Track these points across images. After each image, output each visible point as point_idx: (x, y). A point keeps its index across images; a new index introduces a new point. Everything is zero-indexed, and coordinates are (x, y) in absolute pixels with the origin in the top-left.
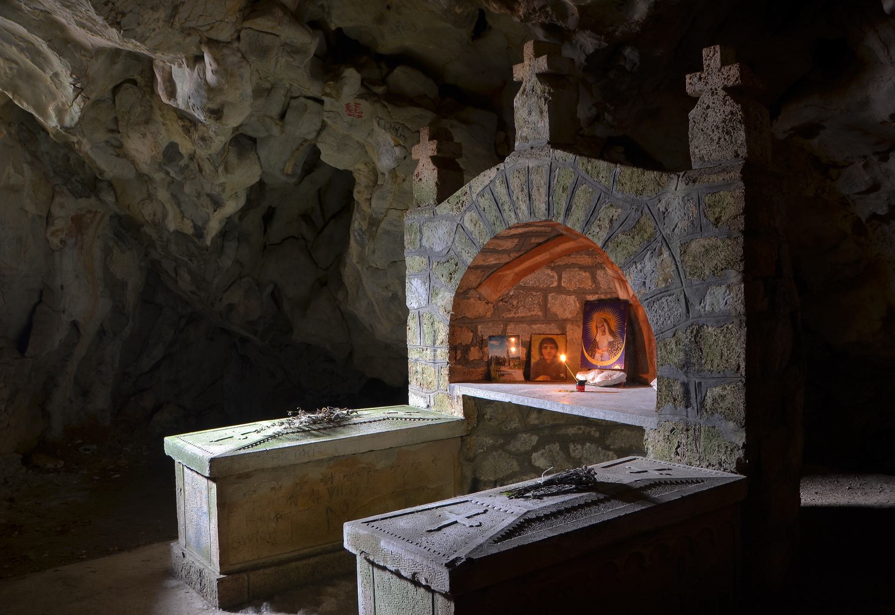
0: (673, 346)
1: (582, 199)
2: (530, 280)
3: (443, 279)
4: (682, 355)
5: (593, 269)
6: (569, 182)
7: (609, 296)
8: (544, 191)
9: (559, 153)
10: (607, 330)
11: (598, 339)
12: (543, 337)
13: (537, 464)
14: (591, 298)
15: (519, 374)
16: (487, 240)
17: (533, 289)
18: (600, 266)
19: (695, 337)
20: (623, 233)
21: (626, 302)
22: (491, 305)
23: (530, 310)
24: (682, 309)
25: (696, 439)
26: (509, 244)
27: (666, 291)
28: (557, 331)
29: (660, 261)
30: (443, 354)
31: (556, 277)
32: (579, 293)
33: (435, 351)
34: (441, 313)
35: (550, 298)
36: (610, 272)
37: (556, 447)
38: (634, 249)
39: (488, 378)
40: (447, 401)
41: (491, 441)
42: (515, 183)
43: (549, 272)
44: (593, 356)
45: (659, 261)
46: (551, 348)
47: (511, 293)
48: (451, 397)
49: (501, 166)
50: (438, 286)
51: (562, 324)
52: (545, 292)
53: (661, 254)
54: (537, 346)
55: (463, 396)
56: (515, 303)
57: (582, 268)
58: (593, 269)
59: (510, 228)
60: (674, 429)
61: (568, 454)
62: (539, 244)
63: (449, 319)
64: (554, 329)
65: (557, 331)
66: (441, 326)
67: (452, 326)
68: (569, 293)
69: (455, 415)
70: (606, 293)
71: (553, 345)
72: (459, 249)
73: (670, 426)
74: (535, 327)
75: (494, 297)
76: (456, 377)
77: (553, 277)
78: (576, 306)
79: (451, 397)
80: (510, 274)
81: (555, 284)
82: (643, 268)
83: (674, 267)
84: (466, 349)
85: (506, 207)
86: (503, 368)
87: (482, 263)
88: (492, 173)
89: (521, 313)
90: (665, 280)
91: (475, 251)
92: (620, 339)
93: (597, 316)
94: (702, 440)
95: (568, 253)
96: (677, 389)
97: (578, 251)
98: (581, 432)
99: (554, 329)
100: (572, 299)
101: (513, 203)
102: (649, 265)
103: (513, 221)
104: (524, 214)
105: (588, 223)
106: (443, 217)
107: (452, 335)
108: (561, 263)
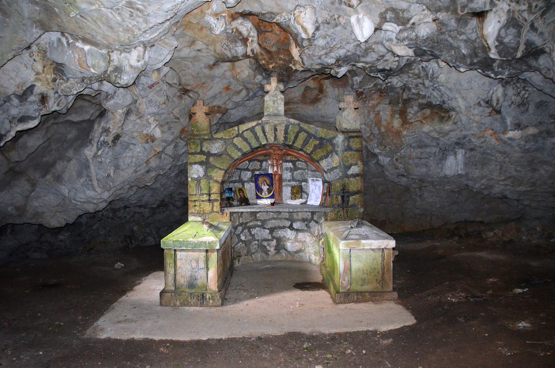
1: (303, 136)
6: (296, 130)
8: (283, 133)
9: (292, 121)
14: (257, 173)
18: (266, 161)
27: (336, 168)
32: (253, 171)
37: (246, 231)
42: (267, 128)
44: (261, 194)
49: (260, 122)
57: (259, 161)
61: (250, 232)
64: (239, 185)
88: (254, 123)
95: (257, 156)
104: (271, 140)
106: (218, 139)
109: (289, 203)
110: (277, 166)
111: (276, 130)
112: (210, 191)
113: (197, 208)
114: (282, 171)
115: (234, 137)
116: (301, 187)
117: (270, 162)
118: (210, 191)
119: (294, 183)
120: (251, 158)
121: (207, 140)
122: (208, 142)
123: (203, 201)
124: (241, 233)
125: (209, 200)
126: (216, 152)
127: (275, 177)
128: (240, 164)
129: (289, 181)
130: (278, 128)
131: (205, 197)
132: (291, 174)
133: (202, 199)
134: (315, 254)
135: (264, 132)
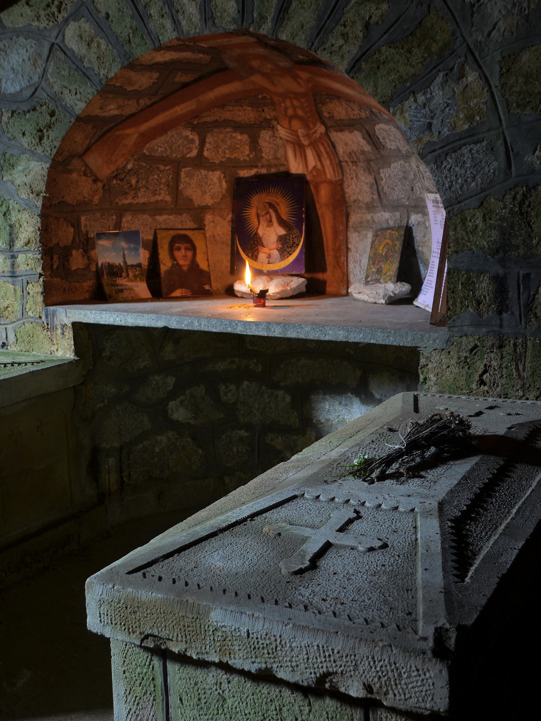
0: (479, 222)
2: (159, 146)
3: (25, 141)
4: (494, 234)
5: (252, 130)
7: (273, 171)
10: (274, 219)
11: (260, 232)
12: (173, 233)
13: (175, 417)
14: (245, 173)
15: (142, 288)
16: (115, 69)
17: (163, 160)
18: (268, 124)
19: (521, 204)
20: (390, 44)
21: (301, 178)
22: (100, 185)
23: (154, 193)
24: (494, 165)
25: (518, 358)
26: (144, 81)
28: (191, 225)
29: (461, 88)
30: (29, 262)
31: (197, 142)
32: (228, 166)
33: (13, 257)
34: (24, 196)
35: (183, 175)
36: (282, 132)
38: (412, 70)
39: (100, 296)
40: (42, 335)
41: (113, 390)
43: (187, 133)
45: (458, 89)
46: (186, 249)
47: (129, 166)
48: (49, 327)
50: (15, 152)
51: (198, 214)
52: (178, 164)
53: (462, 75)
54: (166, 247)
55: (74, 324)
56: (133, 182)
57: (238, 127)
58: (252, 130)
59: (160, 48)
60: (476, 346)
62: (185, 85)
63: (39, 204)
65: (191, 225)
66: (25, 216)
67: (44, 216)
68: (212, 167)
69: (68, 356)
70: (269, 166)
71: (188, 245)
72: (56, 88)
73: (468, 342)
74: (160, 218)
75: (105, 172)
76: (54, 296)
77: (192, 141)
78: (221, 186)
79: (49, 327)
80: (132, 134)
81: (194, 153)
82: (429, 100)
83: (486, 96)
84: (66, 253)
85: (154, 11)
86: (121, 281)
87: (97, 112)
89: (142, 198)
90: (470, 118)
91: (89, 91)
92: (296, 231)
93: (257, 201)
94: (529, 359)
95: (222, 103)
96: (484, 286)
97: (237, 100)
98: (234, 367)
99: (184, 222)
100: (216, 176)
102: (438, 95)
103: (169, 35)
105: (321, 31)
107: (45, 232)
108: (209, 119)
110: (313, 145)
114: (339, 166)
115: (66, 21)
117: (282, 132)
119: (385, 217)
120: (196, 114)
124: (172, 395)
127: (317, 188)
128: (147, 137)
129: (370, 207)
132: (370, 179)
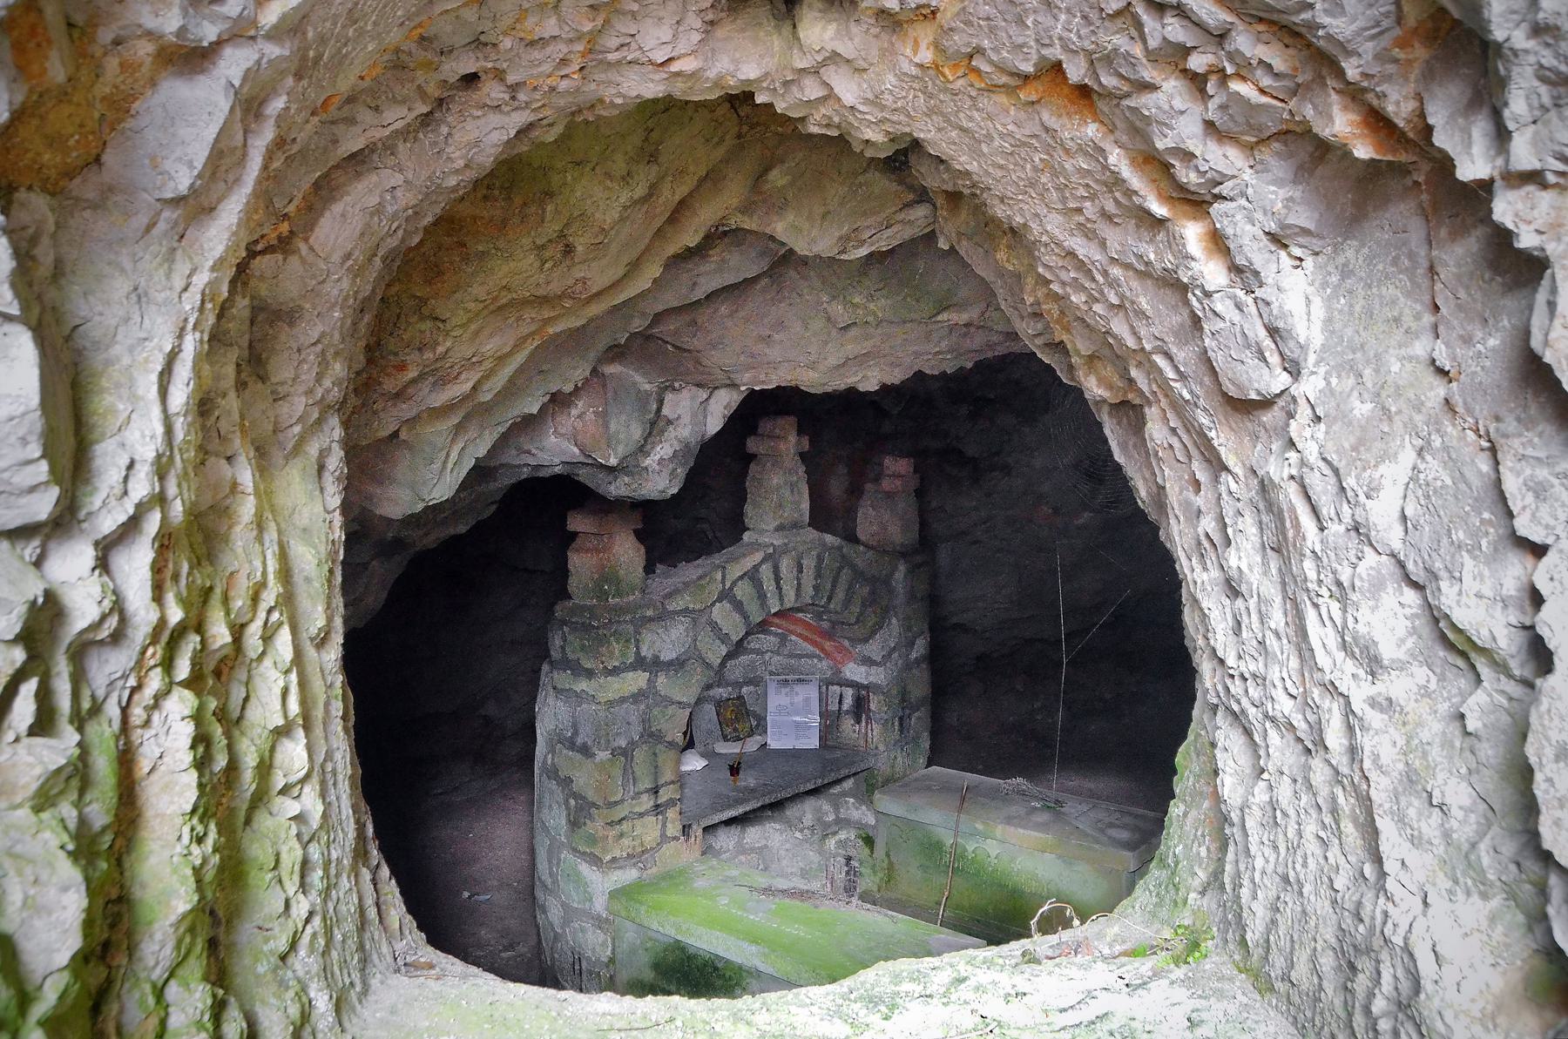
101: (779, 588)
109: (723, 751)
111: (800, 571)
112: (656, 780)
113: (626, 841)
116: (740, 697)
118: (656, 780)
121: (651, 620)
122: (653, 626)
123: (641, 815)
125: (658, 809)
126: (674, 655)
130: (805, 562)
131: (647, 802)
133: (637, 809)
134: (804, 874)
135: (778, 579)
